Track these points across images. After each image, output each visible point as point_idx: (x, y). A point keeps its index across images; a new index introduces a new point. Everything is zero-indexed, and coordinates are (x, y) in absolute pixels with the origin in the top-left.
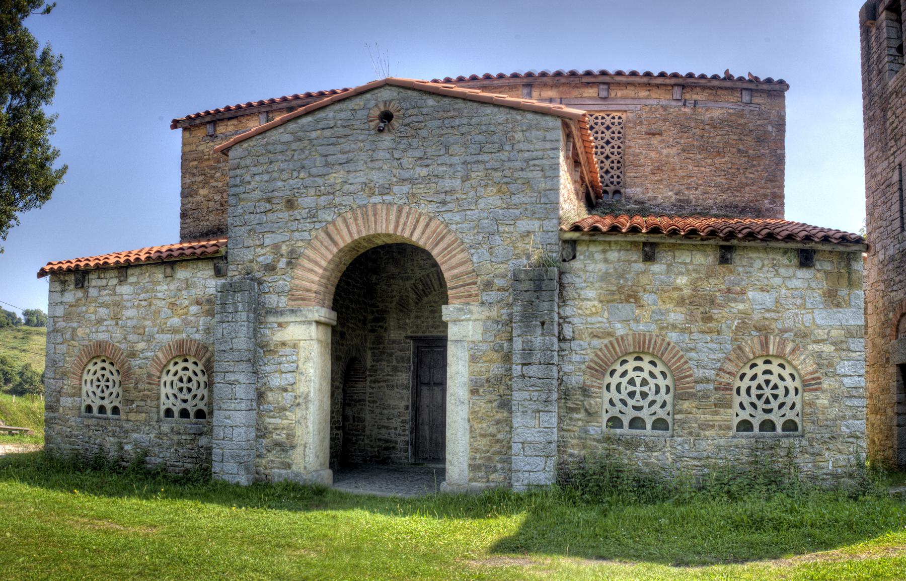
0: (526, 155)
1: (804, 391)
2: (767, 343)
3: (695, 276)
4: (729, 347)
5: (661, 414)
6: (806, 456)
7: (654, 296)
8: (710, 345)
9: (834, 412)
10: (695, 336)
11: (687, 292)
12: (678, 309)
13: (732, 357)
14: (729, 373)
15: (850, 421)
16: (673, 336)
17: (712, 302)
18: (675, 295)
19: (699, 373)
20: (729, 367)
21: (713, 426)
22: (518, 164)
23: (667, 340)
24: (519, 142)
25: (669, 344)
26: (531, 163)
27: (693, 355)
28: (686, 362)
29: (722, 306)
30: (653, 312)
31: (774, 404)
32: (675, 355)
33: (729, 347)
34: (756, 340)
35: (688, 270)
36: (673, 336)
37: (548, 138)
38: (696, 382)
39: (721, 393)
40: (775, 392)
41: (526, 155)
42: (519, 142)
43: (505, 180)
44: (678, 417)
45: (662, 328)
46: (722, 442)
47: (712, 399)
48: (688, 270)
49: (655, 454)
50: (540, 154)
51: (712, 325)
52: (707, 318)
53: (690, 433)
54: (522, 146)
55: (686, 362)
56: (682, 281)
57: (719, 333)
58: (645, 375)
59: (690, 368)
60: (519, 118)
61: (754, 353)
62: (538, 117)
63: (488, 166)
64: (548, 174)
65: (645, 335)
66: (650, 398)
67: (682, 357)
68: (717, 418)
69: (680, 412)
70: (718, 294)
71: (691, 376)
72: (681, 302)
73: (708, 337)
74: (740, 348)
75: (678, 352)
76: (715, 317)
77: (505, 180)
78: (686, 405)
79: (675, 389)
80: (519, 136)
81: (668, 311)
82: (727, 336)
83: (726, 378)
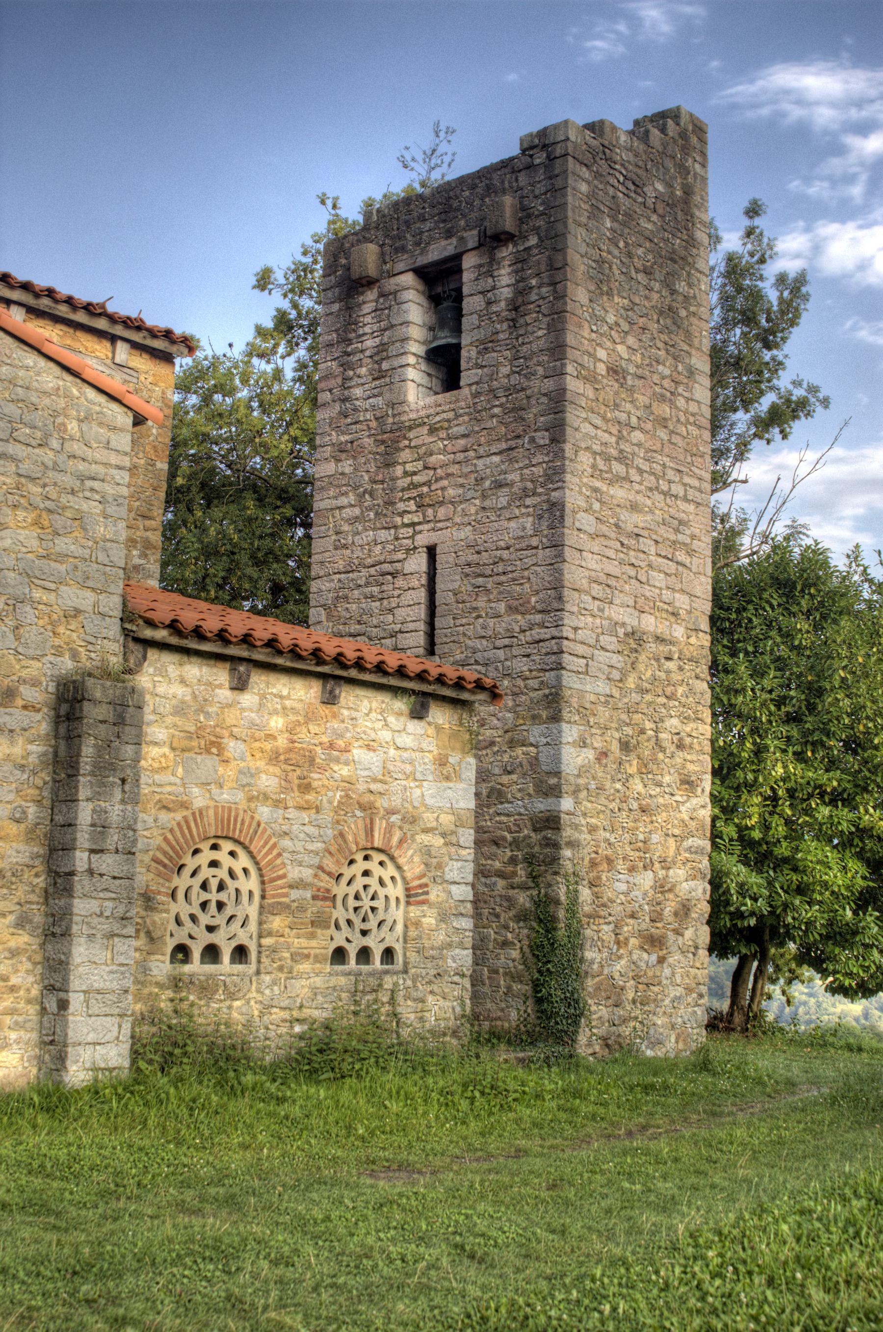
0: (82, 466)
1: (408, 903)
2: (372, 830)
3: (293, 718)
4: (330, 832)
5: (243, 938)
6: (409, 1003)
7: (241, 746)
8: (310, 829)
9: (441, 937)
10: (292, 813)
11: (282, 742)
12: (271, 769)
13: (333, 849)
14: (329, 874)
15: (457, 951)
16: (264, 812)
17: (312, 761)
18: (268, 746)
19: (294, 873)
20: (330, 864)
21: (307, 956)
22: (67, 480)
23: (257, 817)
24: (72, 439)
25: (259, 825)
26: (89, 483)
27: (286, 843)
28: (279, 855)
29: (322, 769)
30: (241, 772)
31: (372, 924)
32: (266, 843)
33: (330, 832)
34: (361, 824)
35: (284, 708)
36: (264, 812)
37: (113, 444)
38: (291, 887)
39: (320, 903)
40: (374, 904)
41: (82, 466)
42: (72, 439)
43: (48, 504)
44: (266, 941)
45: (250, 799)
46: (318, 981)
47: (309, 914)
48: (284, 708)
49: (237, 1004)
50: (100, 470)
51: (310, 797)
52: (306, 787)
53: (281, 969)
54: (76, 447)
55: (279, 855)
56: (277, 723)
57: (318, 810)
58: (222, 873)
59: (284, 864)
60: (75, 391)
61: (357, 844)
62: (102, 399)
63: (25, 467)
64: (110, 510)
65: (230, 809)
66: (229, 911)
67: (274, 846)
68: (314, 943)
69: (270, 934)
70: (319, 750)
71: (284, 876)
72: (274, 758)
73: (305, 816)
74: (342, 835)
75: (270, 838)
76: (315, 784)
77: (48, 504)
78: (277, 923)
79: (263, 897)
80: (73, 427)
81: (259, 771)
82: (327, 816)
83: (326, 882)
